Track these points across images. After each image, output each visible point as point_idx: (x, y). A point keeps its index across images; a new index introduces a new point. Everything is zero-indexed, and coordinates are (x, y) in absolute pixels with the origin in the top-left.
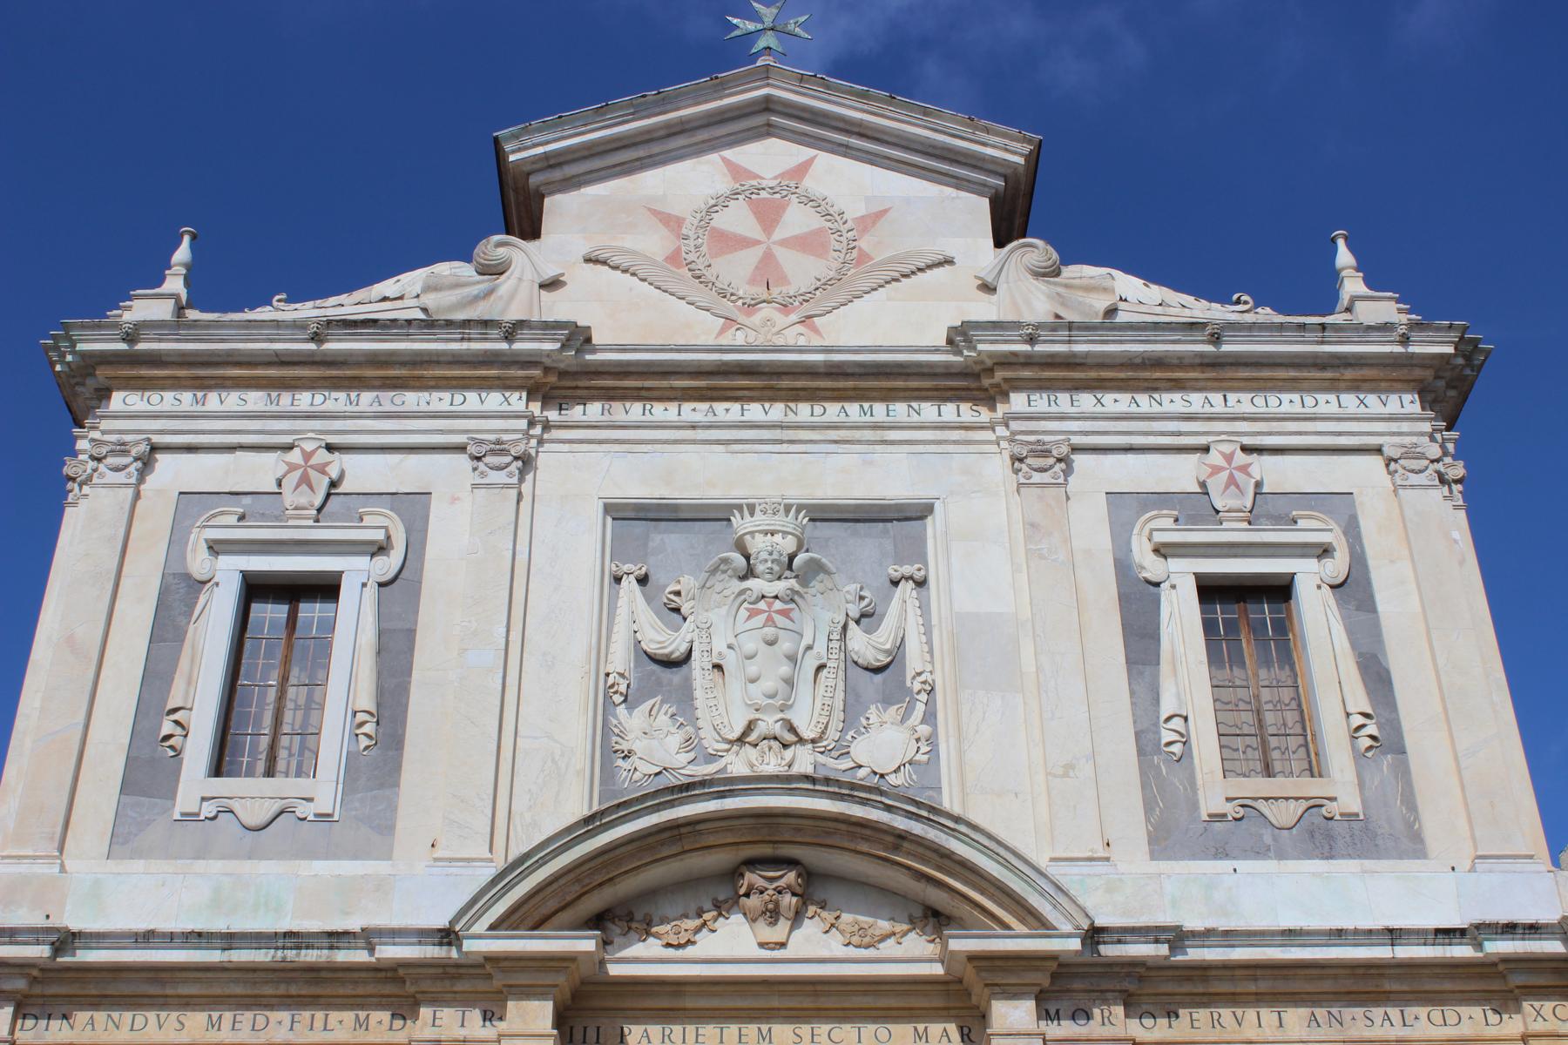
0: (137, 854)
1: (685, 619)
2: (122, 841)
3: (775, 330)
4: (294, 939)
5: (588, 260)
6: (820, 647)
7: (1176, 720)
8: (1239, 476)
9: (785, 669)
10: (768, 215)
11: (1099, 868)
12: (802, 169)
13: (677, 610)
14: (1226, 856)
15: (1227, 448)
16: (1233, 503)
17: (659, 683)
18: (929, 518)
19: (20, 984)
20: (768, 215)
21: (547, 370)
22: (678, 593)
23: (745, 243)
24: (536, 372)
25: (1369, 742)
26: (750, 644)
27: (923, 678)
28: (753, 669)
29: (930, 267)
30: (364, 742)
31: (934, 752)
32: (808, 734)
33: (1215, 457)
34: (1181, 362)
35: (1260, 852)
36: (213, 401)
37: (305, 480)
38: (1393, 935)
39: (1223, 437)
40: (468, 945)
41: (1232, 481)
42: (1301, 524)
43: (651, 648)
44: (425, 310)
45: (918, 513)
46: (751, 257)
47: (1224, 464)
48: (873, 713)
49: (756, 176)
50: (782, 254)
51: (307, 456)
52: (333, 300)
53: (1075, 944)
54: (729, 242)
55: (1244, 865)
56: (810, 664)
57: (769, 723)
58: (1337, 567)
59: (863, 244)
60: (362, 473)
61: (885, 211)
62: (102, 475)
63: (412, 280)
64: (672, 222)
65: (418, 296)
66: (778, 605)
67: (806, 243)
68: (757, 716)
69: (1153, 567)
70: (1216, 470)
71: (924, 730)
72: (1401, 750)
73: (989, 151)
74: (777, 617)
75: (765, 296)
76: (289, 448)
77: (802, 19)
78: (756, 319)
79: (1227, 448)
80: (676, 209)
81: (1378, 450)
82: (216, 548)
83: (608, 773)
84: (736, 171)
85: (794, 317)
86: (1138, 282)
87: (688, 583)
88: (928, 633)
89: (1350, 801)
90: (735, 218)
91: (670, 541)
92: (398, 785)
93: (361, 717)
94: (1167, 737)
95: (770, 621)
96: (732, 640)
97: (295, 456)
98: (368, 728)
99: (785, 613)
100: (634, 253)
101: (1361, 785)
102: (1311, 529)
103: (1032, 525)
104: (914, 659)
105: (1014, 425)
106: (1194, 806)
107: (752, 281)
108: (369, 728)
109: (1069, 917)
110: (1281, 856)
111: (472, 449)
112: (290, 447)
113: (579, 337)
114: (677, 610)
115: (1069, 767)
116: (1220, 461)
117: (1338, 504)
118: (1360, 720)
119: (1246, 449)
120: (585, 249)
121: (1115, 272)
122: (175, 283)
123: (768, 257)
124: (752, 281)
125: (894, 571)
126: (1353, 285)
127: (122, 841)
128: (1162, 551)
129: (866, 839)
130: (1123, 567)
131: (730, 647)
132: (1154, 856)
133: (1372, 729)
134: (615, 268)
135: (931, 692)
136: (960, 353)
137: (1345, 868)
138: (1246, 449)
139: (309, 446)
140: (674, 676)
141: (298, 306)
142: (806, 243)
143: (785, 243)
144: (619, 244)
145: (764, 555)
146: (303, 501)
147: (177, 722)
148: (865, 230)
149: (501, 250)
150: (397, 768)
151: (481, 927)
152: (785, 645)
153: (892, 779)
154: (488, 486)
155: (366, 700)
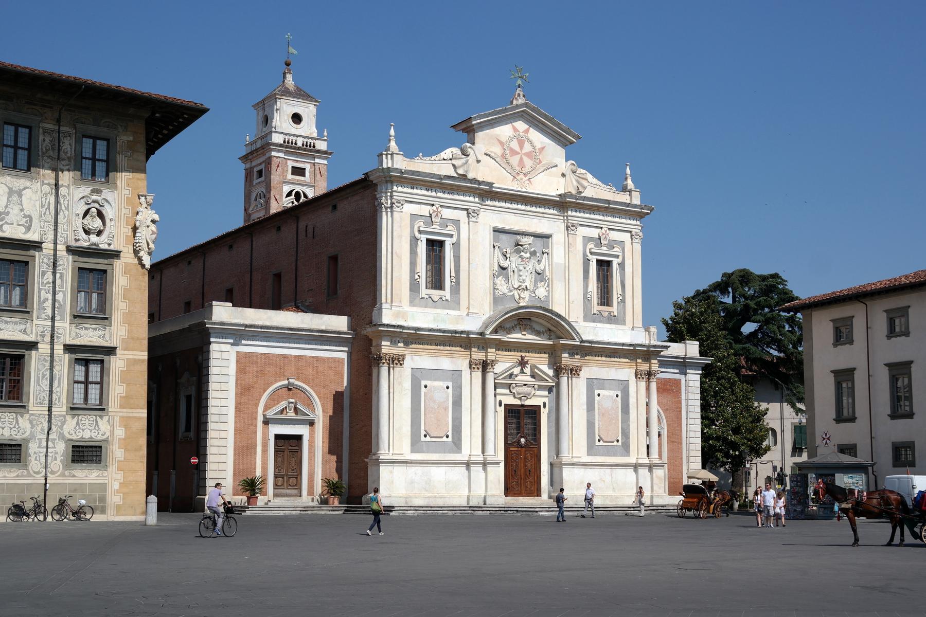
0: (414, 306)
1: (507, 258)
2: (412, 302)
3: (523, 181)
4: (456, 332)
5: (485, 154)
6: (531, 269)
7: (590, 293)
8: (607, 236)
9: (526, 274)
10: (521, 144)
11: (576, 324)
12: (527, 131)
13: (505, 256)
14: (595, 322)
15: (606, 229)
16: (605, 242)
17: (502, 273)
18: (550, 238)
19: (406, 336)
20: (521, 144)
21: (484, 190)
22: (506, 252)
23: (517, 153)
24: (482, 192)
25: (620, 300)
26: (521, 268)
27: (548, 277)
28: (521, 273)
29: (553, 167)
30: (453, 284)
31: (549, 294)
32: (528, 288)
33: (603, 231)
34: (601, 207)
35: (600, 322)
36: (415, 191)
37: (437, 215)
38: (623, 345)
39: (605, 226)
40: (487, 336)
41: (606, 237)
42: (616, 249)
43: (502, 265)
44: (454, 166)
45: (548, 237)
46: (517, 158)
47: (604, 232)
48: (539, 283)
49: (519, 131)
50: (523, 157)
51: (437, 209)
52: (434, 158)
53: (579, 343)
54: (513, 152)
55: (599, 325)
56: (529, 272)
57: (524, 286)
58: (620, 260)
59: (540, 157)
60: (447, 213)
61: (544, 147)
62: (395, 208)
63: (447, 153)
64: (501, 143)
65: (451, 159)
66: (527, 260)
67: (529, 155)
68: (521, 284)
69: (590, 257)
70: (603, 234)
71: (547, 289)
72: (625, 302)
73: (570, 137)
74: (527, 263)
75: (521, 171)
76: (433, 205)
77: (527, 74)
78: (519, 178)
79: (606, 229)
80: (504, 140)
81: (631, 232)
82: (420, 232)
83: (494, 293)
84: (515, 129)
85: (527, 178)
86: (591, 176)
87: (509, 251)
88: (549, 266)
89: (616, 314)
90: (515, 145)
91: (503, 237)
92: (459, 294)
93: (452, 278)
94: (589, 296)
95: (525, 263)
96: (517, 266)
97: (434, 208)
98: (454, 280)
99: (528, 261)
100: (495, 153)
101: (617, 309)
102: (617, 250)
103: (571, 244)
104: (547, 273)
105: (569, 218)
106: (591, 311)
107: (518, 166)
108: (454, 280)
109: (578, 338)
110: (603, 323)
111: (470, 211)
112: (433, 205)
113: (490, 184)
114: (505, 256)
115: (573, 301)
116: (604, 232)
117: (621, 244)
118: (619, 296)
119: (609, 229)
120: (484, 151)
121: (587, 172)
122: (393, 144)
123: (521, 159)
124: (518, 166)
125: (545, 250)
126: (630, 184)
127: (412, 302)
128: (591, 253)
129: (545, 318)
130: (585, 255)
131: (516, 267)
132: (584, 321)
133: (621, 298)
134: (492, 157)
135: (549, 280)
136: (562, 198)
137: (613, 326)
138: (609, 229)
139: (437, 206)
140: (505, 271)
141: (426, 158)
142: (529, 155)
143: (525, 154)
144: (491, 150)
145: (526, 248)
146: (436, 220)
147: (419, 276)
148: (540, 153)
149: (469, 150)
150: (459, 290)
151: (488, 333)
152: (527, 269)
153: (542, 299)
154: (473, 221)
155: (453, 274)
